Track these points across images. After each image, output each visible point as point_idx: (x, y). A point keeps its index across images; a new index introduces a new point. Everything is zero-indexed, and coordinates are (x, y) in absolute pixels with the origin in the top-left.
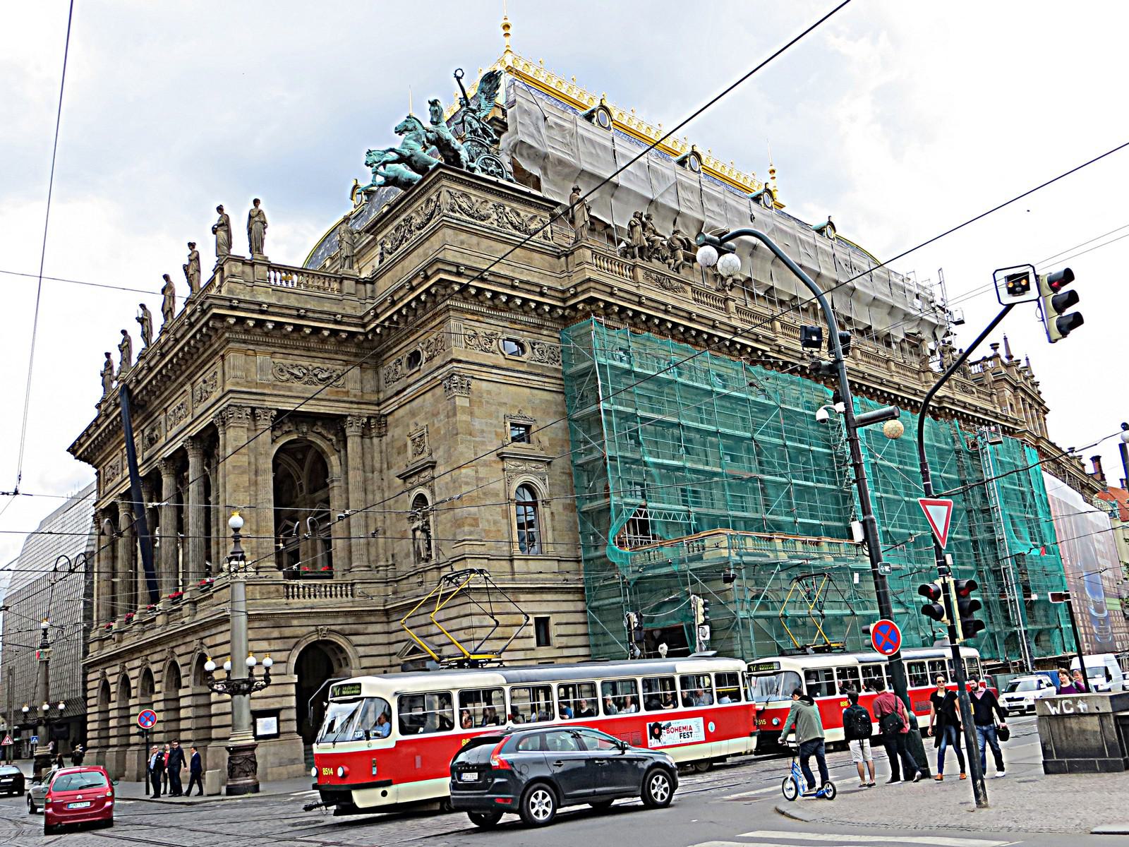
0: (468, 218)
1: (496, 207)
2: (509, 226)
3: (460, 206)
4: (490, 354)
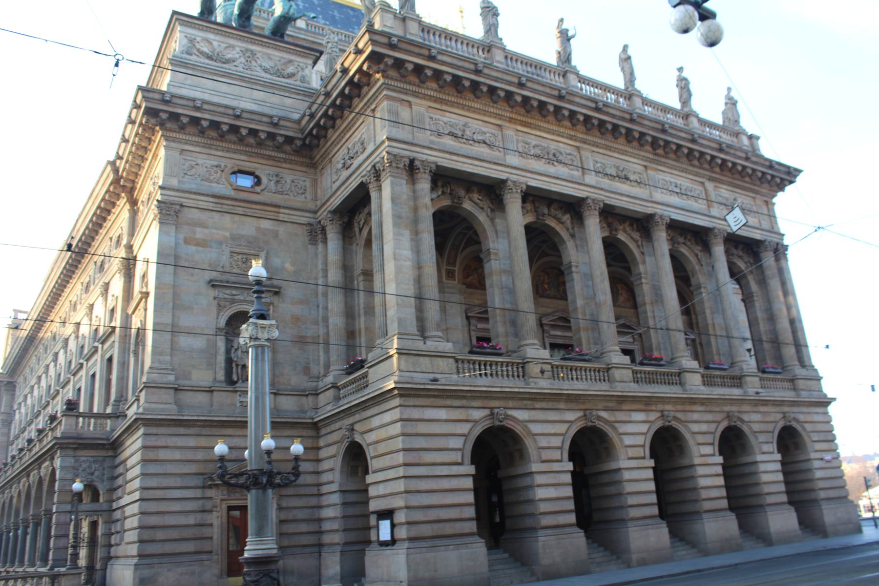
0: (207, 61)
1: (244, 51)
2: (258, 69)
3: (198, 50)
4: (215, 185)
